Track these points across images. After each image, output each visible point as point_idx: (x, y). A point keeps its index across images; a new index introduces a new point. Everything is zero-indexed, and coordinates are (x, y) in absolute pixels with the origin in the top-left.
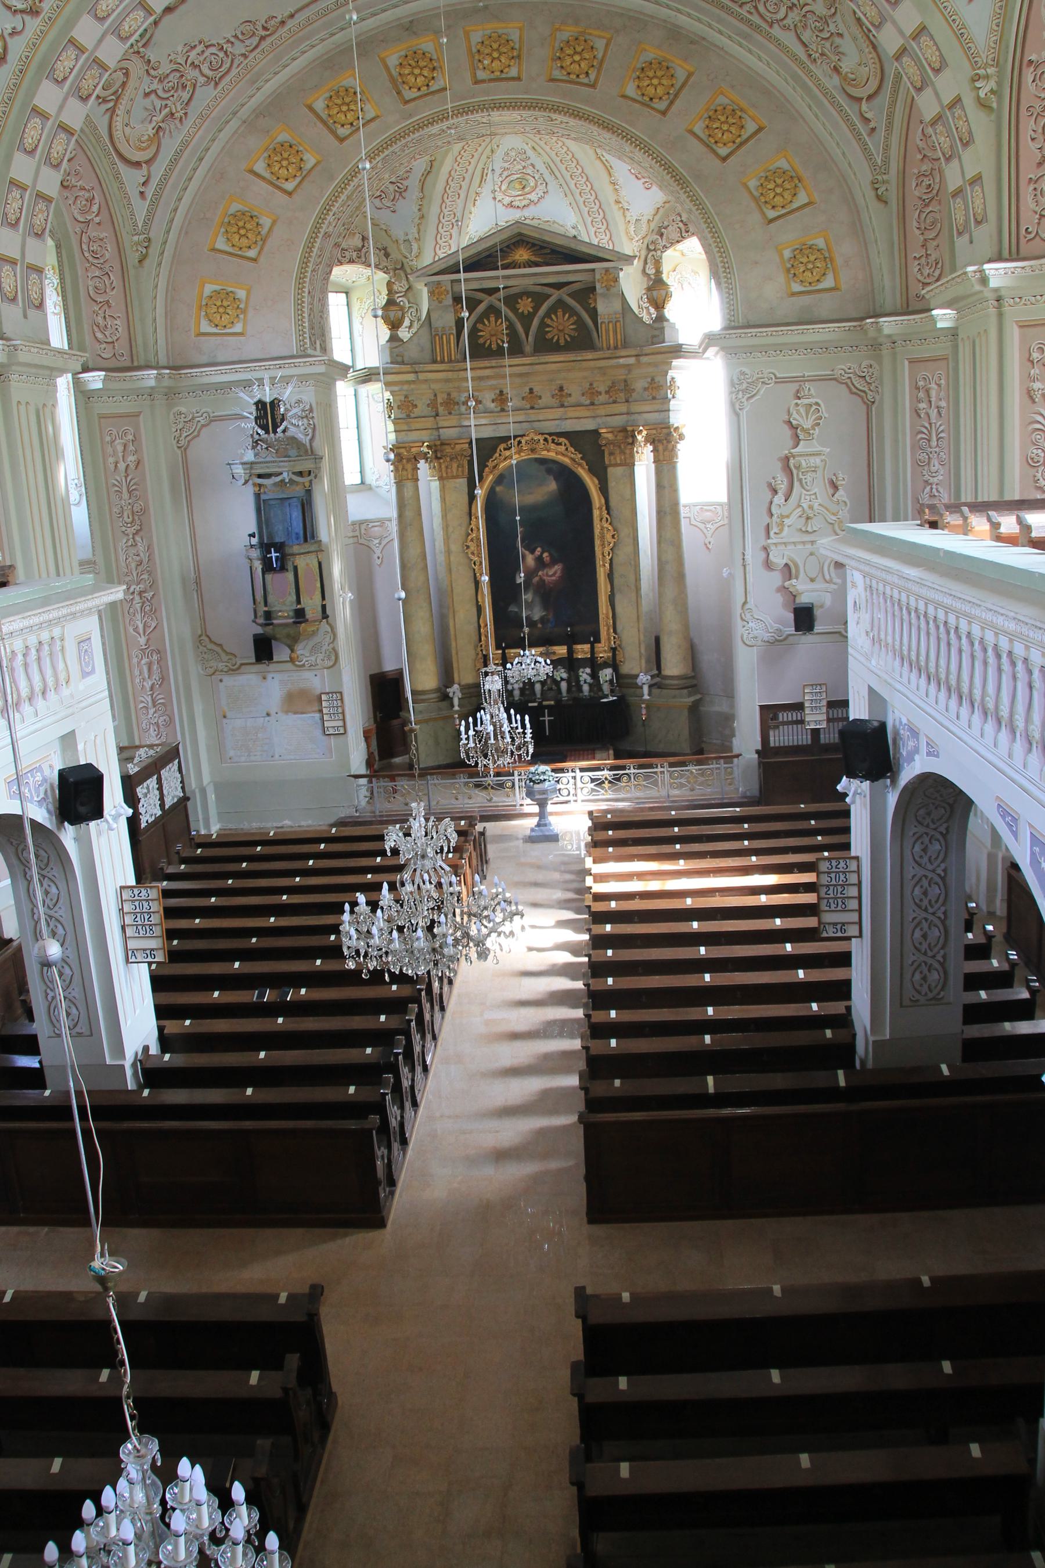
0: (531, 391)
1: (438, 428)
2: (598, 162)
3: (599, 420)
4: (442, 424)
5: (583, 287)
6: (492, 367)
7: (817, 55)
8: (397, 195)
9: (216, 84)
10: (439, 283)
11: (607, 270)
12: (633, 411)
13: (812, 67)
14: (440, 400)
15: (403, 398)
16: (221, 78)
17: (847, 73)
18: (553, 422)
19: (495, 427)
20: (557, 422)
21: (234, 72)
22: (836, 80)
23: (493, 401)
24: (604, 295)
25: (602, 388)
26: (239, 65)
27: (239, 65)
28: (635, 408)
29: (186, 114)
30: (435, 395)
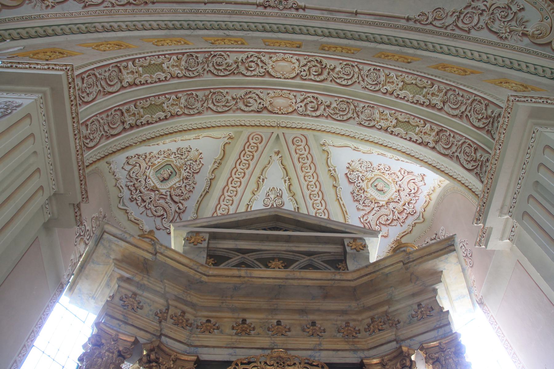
0: (279, 323)
1: (162, 334)
2: (337, 203)
3: (361, 354)
4: (165, 331)
5: (332, 258)
6: (240, 277)
7: (506, 35)
8: (177, 215)
9: (85, 7)
10: (198, 233)
11: (355, 239)
12: (402, 337)
13: (506, 42)
14: (170, 312)
15: (130, 294)
16: (90, 5)
17: (533, 33)
18: (305, 352)
19: (231, 351)
20: (310, 353)
21: (101, 8)
22: (526, 40)
23: (233, 328)
24: (354, 257)
25: (362, 328)
26: (106, 7)
27: (106, 7)
28: (404, 333)
29: (53, 7)
30: (168, 309)
